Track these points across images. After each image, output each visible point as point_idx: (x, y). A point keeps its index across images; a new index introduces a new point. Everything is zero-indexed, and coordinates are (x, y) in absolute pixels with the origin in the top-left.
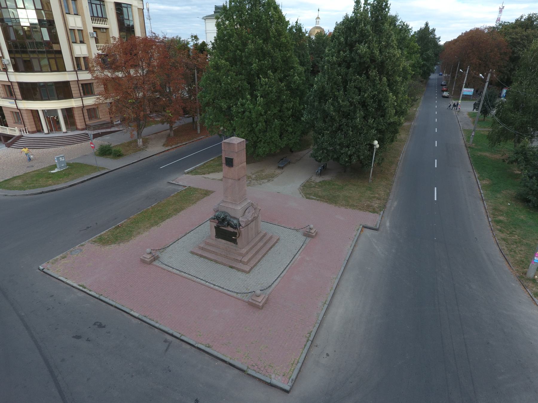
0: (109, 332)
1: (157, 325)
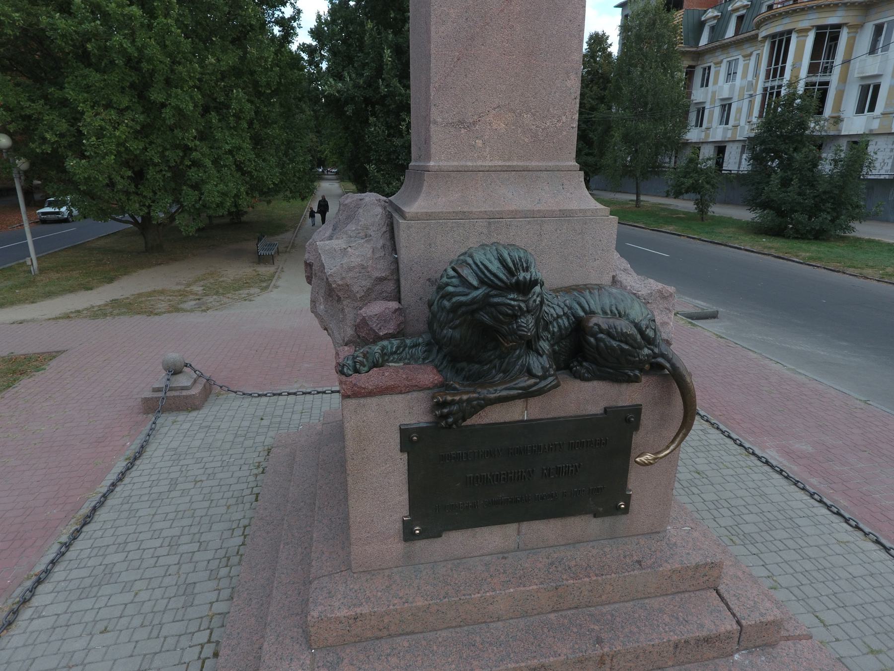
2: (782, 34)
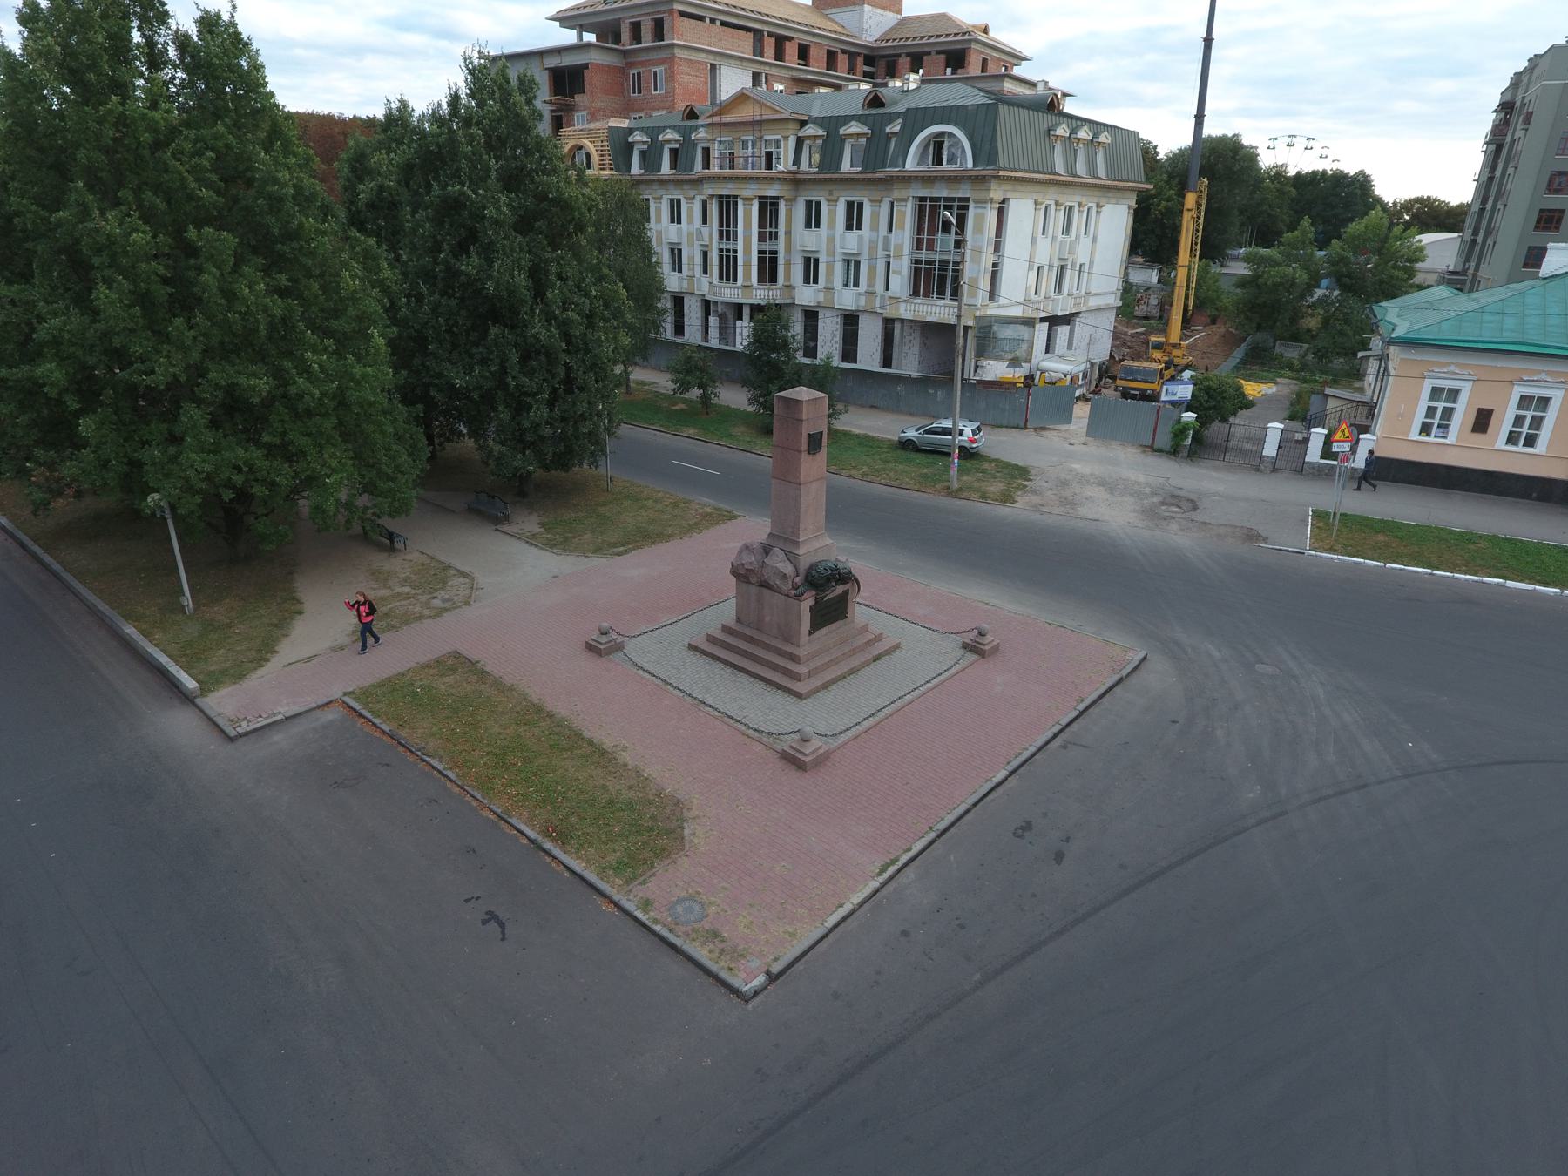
0: (1045, 815)
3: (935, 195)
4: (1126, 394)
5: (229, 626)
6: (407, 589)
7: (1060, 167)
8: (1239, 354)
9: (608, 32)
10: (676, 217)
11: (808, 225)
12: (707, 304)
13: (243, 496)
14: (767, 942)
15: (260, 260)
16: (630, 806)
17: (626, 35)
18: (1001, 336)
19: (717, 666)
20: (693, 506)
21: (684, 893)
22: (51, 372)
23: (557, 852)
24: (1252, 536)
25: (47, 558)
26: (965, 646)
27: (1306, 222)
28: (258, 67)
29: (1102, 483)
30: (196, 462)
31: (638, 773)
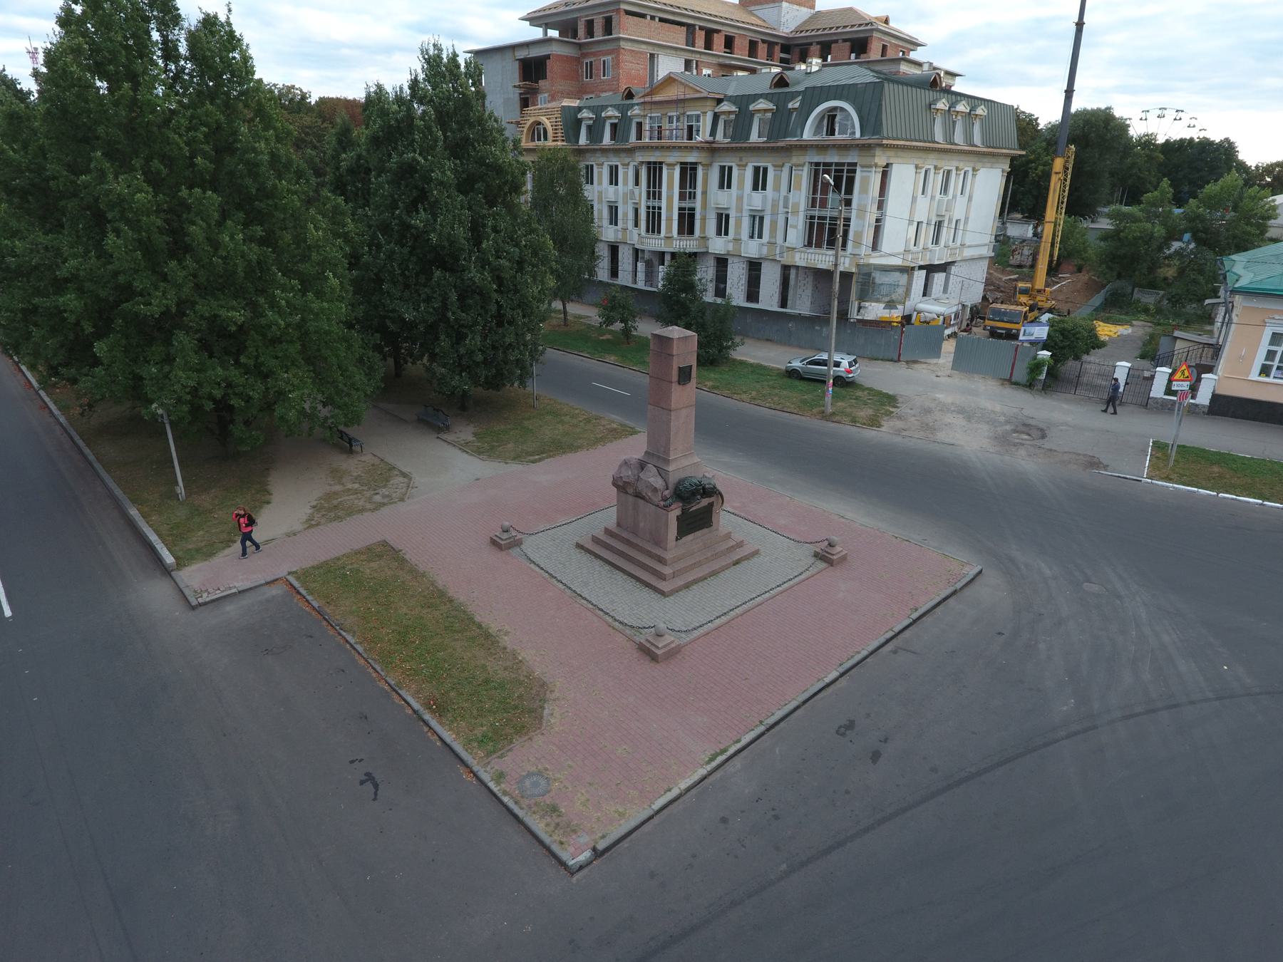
0: (868, 715)
1: (865, 653)
2: (655, 163)
3: (828, 160)
4: (994, 334)
5: (211, 511)
6: (356, 486)
7: (939, 137)
8: (1098, 300)
9: (568, 28)
10: (614, 180)
11: (721, 186)
12: (636, 251)
13: (223, 406)
14: (598, 819)
15: (241, 215)
16: (502, 686)
17: (581, 31)
18: (878, 281)
19: (598, 562)
20: (603, 422)
21: (534, 769)
22: (70, 300)
23: (434, 723)
24: (1094, 464)
25: (87, 451)
26: (816, 555)
27: (1165, 183)
28: (246, 59)
29: (961, 411)
30: (183, 378)
31: (514, 655)
